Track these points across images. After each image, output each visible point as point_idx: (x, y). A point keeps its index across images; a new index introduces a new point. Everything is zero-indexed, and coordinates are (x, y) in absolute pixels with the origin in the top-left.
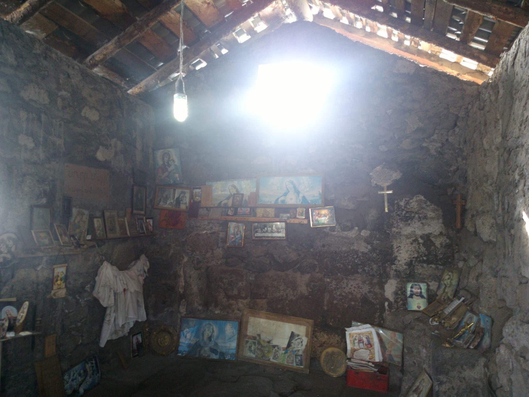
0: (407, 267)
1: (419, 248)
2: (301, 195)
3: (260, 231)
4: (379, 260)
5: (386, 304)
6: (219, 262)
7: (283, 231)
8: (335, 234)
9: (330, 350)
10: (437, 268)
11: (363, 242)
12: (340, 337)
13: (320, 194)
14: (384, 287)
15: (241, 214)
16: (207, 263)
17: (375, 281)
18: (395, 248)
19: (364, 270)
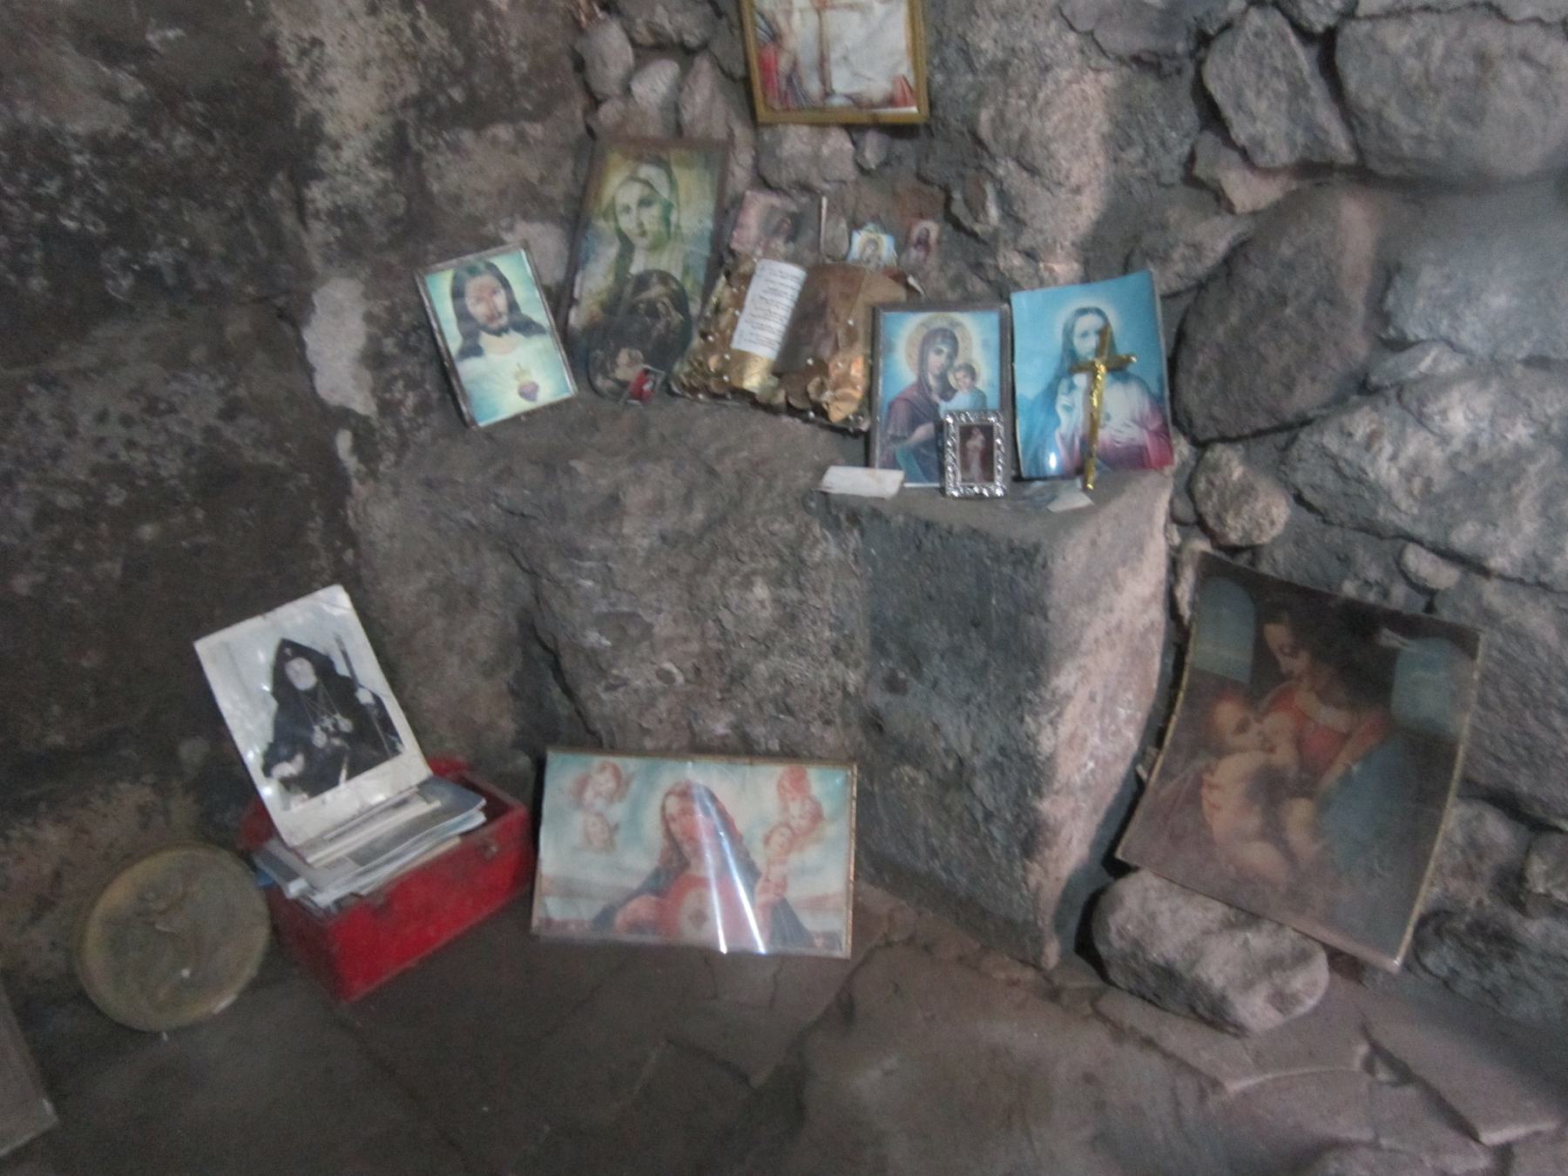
0: (387, 175)
1: (419, 35)
4: (224, 169)
5: (344, 442)
9: (119, 895)
10: (521, 136)
11: (68, 48)
12: (148, 778)
14: (302, 345)
17: (238, 325)
18: (292, 60)
19: (150, 276)
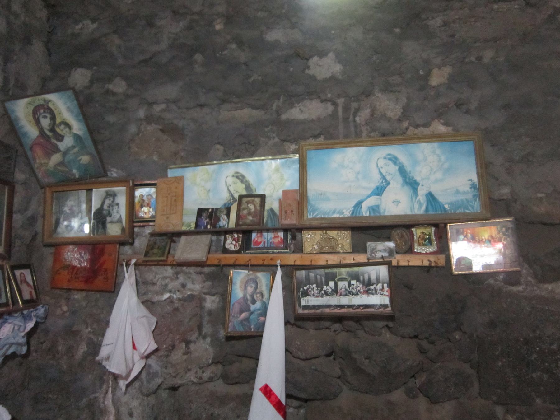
2: (422, 192)
3: (317, 292)
6: (206, 375)
7: (382, 289)
8: (519, 291)
13: (473, 186)
15: (261, 246)
16: (175, 377)
